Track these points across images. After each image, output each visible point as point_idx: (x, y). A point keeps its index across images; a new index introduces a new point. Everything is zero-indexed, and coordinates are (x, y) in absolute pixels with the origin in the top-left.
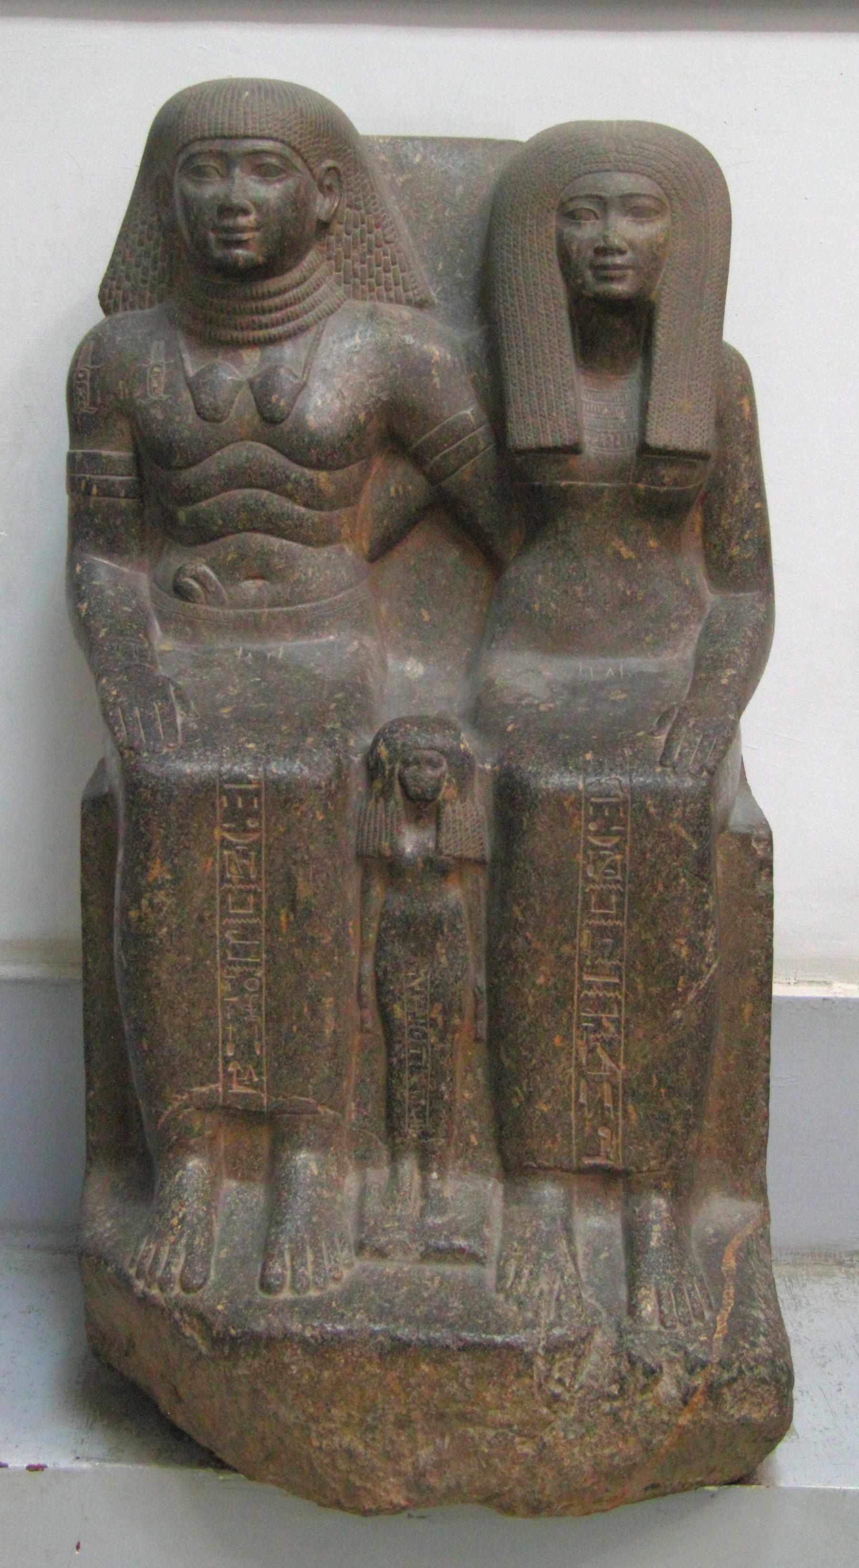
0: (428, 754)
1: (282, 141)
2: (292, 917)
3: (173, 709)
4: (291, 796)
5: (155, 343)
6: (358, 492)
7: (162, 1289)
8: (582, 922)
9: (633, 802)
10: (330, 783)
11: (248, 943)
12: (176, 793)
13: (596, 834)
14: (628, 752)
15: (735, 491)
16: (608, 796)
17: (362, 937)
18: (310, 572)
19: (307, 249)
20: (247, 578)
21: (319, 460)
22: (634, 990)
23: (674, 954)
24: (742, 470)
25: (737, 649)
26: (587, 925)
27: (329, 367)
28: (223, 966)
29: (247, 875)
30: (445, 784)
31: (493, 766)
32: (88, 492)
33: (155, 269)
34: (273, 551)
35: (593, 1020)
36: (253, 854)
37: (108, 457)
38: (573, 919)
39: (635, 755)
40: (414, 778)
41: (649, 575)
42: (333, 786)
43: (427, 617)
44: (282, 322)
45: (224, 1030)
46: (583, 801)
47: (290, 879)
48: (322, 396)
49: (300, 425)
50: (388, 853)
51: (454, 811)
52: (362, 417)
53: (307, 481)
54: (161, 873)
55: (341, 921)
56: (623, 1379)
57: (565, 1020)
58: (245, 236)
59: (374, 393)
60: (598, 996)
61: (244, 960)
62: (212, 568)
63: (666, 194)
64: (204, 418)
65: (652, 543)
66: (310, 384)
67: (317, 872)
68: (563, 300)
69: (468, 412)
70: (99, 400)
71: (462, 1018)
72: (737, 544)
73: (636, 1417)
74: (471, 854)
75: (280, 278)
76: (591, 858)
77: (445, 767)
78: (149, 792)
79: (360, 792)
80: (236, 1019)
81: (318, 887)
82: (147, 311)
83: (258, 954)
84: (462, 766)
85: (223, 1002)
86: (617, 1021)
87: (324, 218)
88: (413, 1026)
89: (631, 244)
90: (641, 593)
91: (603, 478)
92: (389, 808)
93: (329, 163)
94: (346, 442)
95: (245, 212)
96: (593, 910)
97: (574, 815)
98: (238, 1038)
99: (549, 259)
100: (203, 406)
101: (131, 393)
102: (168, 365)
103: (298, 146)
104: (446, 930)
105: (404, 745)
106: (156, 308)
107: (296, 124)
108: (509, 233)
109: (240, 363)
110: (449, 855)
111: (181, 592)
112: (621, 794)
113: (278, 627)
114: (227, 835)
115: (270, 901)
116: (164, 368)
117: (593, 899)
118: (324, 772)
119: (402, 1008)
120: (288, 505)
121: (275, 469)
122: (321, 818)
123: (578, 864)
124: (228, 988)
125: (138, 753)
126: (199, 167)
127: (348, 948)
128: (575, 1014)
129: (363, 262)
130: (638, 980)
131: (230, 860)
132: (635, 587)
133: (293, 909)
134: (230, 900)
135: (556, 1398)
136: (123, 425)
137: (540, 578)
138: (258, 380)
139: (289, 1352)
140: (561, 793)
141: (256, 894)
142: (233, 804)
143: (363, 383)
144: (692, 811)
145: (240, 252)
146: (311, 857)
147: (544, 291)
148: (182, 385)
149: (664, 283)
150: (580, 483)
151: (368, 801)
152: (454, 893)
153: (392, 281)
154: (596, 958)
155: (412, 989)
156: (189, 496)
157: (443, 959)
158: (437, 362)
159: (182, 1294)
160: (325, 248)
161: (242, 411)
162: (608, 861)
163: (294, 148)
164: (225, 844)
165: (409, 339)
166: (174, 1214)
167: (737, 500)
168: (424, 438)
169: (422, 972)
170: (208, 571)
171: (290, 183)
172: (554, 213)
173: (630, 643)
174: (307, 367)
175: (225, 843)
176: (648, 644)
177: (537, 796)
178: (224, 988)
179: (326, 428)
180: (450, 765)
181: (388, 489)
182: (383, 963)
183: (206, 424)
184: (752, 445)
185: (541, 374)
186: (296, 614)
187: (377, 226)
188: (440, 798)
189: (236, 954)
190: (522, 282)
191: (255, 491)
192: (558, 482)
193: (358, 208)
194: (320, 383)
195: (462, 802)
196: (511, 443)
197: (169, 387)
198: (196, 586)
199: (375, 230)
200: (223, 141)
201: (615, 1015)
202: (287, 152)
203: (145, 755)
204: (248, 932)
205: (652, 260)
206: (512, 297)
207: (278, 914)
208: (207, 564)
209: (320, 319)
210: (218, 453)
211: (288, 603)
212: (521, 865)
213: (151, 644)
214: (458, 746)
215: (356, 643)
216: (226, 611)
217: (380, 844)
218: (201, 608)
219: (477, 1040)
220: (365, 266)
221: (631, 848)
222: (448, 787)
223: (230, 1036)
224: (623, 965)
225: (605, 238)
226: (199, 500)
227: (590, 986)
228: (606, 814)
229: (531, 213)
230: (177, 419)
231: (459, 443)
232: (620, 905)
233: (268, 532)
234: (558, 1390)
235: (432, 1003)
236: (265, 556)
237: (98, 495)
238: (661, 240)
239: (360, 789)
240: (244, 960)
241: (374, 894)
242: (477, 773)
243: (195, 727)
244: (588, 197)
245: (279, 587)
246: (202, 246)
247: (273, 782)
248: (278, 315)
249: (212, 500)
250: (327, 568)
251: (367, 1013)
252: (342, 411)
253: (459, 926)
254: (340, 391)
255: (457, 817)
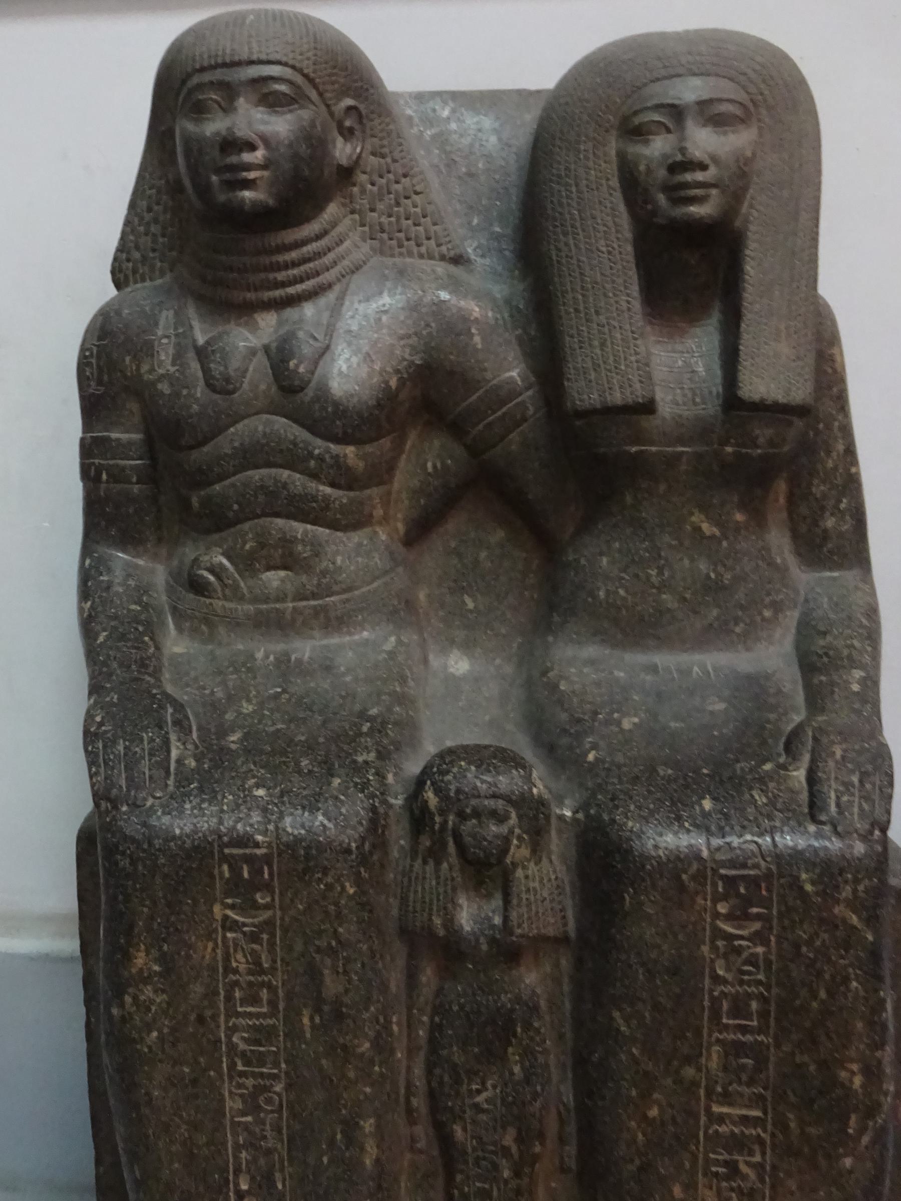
0: (490, 803)
1: (293, 67)
2: (317, 1020)
3: (166, 743)
4: (312, 864)
5: (164, 313)
6: (391, 468)
8: (710, 1036)
9: (781, 875)
10: (363, 844)
11: (262, 1049)
12: (162, 861)
13: (729, 917)
14: (761, 799)
15: (828, 453)
16: (744, 866)
17: (409, 1035)
18: (339, 559)
19: (328, 200)
20: (269, 568)
21: (345, 433)
22: (785, 1128)
23: (842, 1085)
24: (836, 430)
25: (856, 643)
26: (718, 1041)
27: (355, 328)
28: (231, 1078)
29: (258, 963)
30: (515, 842)
31: (575, 812)
32: (97, 479)
33: (163, 236)
34: (296, 538)
35: (726, 1163)
37: (118, 440)
38: (698, 1032)
39: (772, 803)
40: (474, 836)
41: (736, 553)
42: (367, 846)
43: (470, 605)
44: (301, 280)
45: (236, 1157)
46: (709, 873)
47: (314, 973)
48: (348, 360)
49: (323, 393)
51: (527, 877)
52: (393, 383)
53: (332, 457)
54: (146, 964)
55: (382, 1020)
57: (687, 1165)
59: (407, 356)
60: (732, 1133)
61: (256, 1070)
62: (229, 558)
63: (752, 100)
64: (214, 391)
65: (739, 517)
66: (332, 347)
67: (347, 960)
68: (627, 233)
69: (514, 374)
70: (106, 378)
71: (542, 1144)
72: (832, 514)
74: (551, 931)
75: (296, 229)
76: (722, 950)
77: (514, 819)
78: (128, 861)
79: (402, 847)
80: (249, 1145)
81: (350, 981)
82: (159, 282)
83: (276, 1064)
84: (534, 814)
85: (233, 1123)
86: (759, 1167)
87: (344, 162)
88: (480, 1153)
89: (715, 159)
90: (728, 576)
91: (680, 441)
92: (442, 874)
93: (349, 102)
94: (377, 412)
95: (252, 148)
96: (725, 1021)
97: (697, 893)
98: (253, 1168)
99: (609, 187)
100: (213, 378)
102: (177, 335)
103: (312, 75)
104: (519, 1030)
105: (458, 791)
106: (168, 277)
107: (308, 51)
108: (559, 163)
109: (254, 328)
110: (522, 936)
111: (197, 587)
112: (763, 863)
113: (304, 623)
114: (229, 912)
115: (289, 997)
116: (173, 338)
117: (725, 1006)
118: (354, 828)
119: (465, 1129)
121: (295, 445)
122: (351, 891)
123: (704, 958)
124: (239, 1105)
125: (115, 807)
126: (200, 100)
127: (392, 1052)
128: (701, 1156)
129: (390, 216)
130: (791, 1116)
131: (236, 945)
132: (720, 569)
133: (318, 1010)
134: (237, 994)
136: (134, 406)
137: (605, 560)
138: (274, 345)
140: (678, 863)
141: (269, 986)
142: (235, 870)
143: (393, 345)
144: (866, 891)
145: (247, 194)
146: (339, 942)
147: (605, 225)
148: (191, 355)
149: (751, 206)
150: (654, 449)
151: (413, 859)
152: (531, 978)
153: (423, 236)
154: (730, 1084)
155: (477, 1107)
156: (202, 478)
157: (517, 1069)
158: (476, 319)
160: (348, 201)
161: (256, 378)
162: (745, 955)
163: (306, 76)
164: (229, 925)
165: (444, 295)
167: (830, 464)
168: (464, 404)
169: (489, 1084)
170: (225, 562)
171: (305, 114)
172: (614, 132)
173: (716, 635)
174: (330, 331)
175: (228, 924)
176: (738, 635)
177: (643, 866)
178: (232, 1104)
179: (352, 396)
180: (520, 817)
181: (426, 464)
182: (437, 1071)
183: (216, 397)
184: (841, 401)
185: (605, 321)
186: (325, 609)
187: (405, 176)
188: (508, 860)
189: (247, 1063)
190: (577, 217)
191: (273, 471)
192: (627, 448)
193: (383, 156)
194: (345, 345)
195: (536, 864)
196: (569, 404)
197: (178, 358)
198: (211, 578)
199: (403, 180)
200: (225, 70)
201: (757, 1158)
202: (299, 79)
203: (125, 808)
204: (261, 1035)
205: (738, 181)
206: (565, 234)
207: (299, 1014)
208: (223, 554)
209: (343, 276)
210: (232, 429)
211: (314, 596)
212: (623, 957)
213: (157, 648)
214: (530, 789)
215: (393, 639)
216: (246, 607)
217: (430, 920)
218: (218, 604)
219: (563, 1170)
220: (393, 219)
221: (778, 937)
222: (518, 847)
223: (244, 1166)
224: (768, 1095)
225: (683, 150)
226: (213, 483)
227: (721, 1119)
228: (742, 890)
229: (587, 136)
230: (185, 392)
231: (504, 410)
232: (764, 1015)
233: (289, 516)
235: (504, 1128)
236: (287, 542)
237: (107, 482)
238: (749, 154)
239: (402, 842)
240: (256, 1070)
241: (424, 979)
242: (554, 821)
243: (193, 764)
244: (659, 107)
245: (304, 578)
246: (203, 191)
247: (287, 845)
248: (295, 271)
249: (227, 482)
250: (354, 555)
252: (370, 377)
253: (536, 1024)
254: (368, 354)
255: (531, 885)
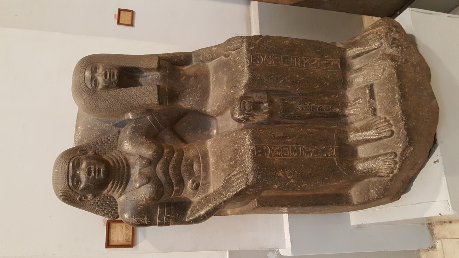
7: (397, 164)
29: (278, 150)
36: (273, 148)
47: (279, 138)
50: (268, 115)
56: (397, 45)
58: (97, 168)
70: (143, 215)
73: (405, 43)
83: (299, 147)
101: (142, 205)
115: (285, 144)
120: (173, 159)
133: (286, 137)
135: (405, 60)
139: (410, 124)
159: (398, 157)
164: (271, 155)
166: (372, 166)
178: (309, 157)
191: (170, 168)
211: (199, 159)
227: (297, 65)
232: (277, 56)
234: (404, 60)
236: (187, 165)
251: (309, 122)
